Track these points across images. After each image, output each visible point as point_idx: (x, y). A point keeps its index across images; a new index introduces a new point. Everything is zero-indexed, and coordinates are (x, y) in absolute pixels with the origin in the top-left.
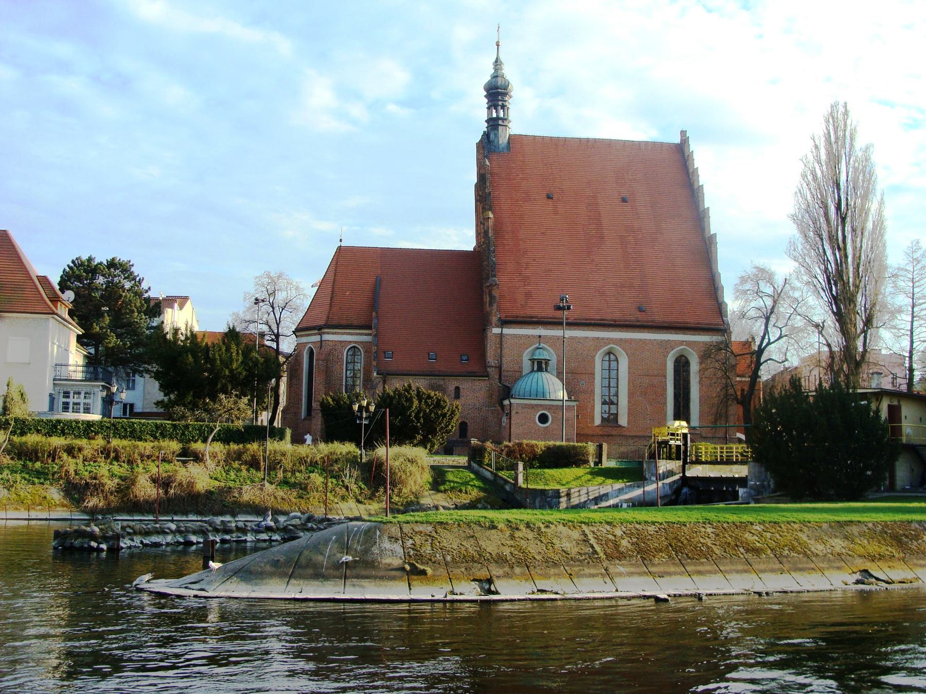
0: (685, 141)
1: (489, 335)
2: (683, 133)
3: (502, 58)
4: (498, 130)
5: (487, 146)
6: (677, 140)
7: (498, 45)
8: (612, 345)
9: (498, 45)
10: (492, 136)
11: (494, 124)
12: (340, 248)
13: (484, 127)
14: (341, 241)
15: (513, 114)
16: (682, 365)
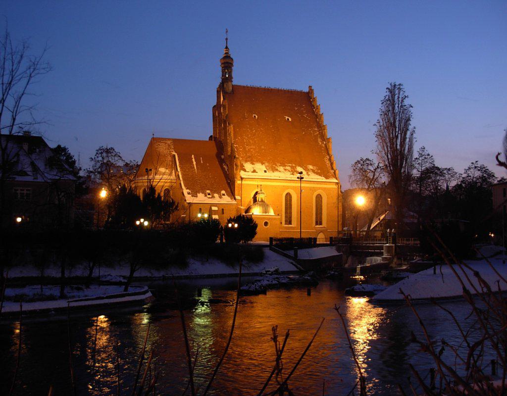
0: (311, 90)
1: (236, 183)
2: (310, 87)
3: (229, 47)
4: (228, 82)
5: (222, 88)
6: (306, 90)
7: (227, 39)
8: (290, 190)
9: (227, 39)
10: (225, 85)
11: (226, 79)
12: (153, 139)
13: (220, 81)
14: (153, 135)
15: (234, 74)
16: (319, 197)
